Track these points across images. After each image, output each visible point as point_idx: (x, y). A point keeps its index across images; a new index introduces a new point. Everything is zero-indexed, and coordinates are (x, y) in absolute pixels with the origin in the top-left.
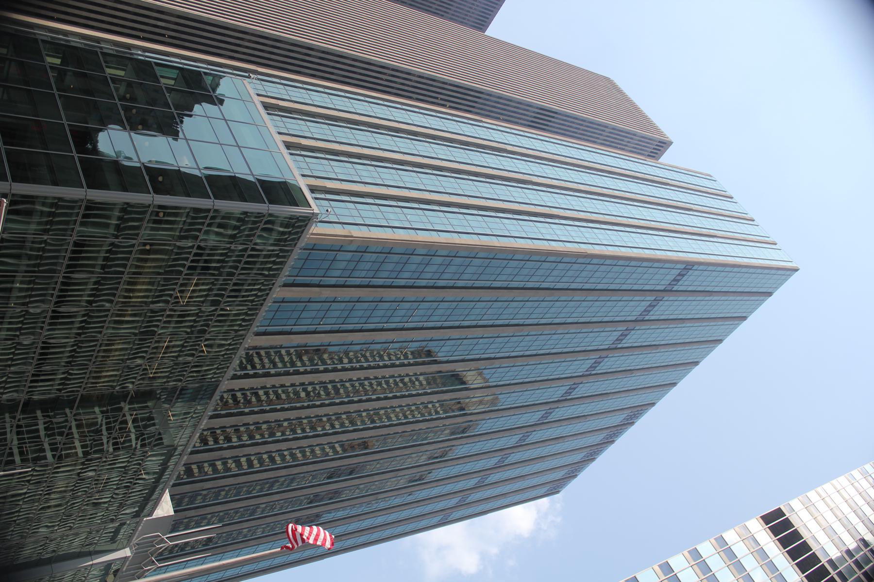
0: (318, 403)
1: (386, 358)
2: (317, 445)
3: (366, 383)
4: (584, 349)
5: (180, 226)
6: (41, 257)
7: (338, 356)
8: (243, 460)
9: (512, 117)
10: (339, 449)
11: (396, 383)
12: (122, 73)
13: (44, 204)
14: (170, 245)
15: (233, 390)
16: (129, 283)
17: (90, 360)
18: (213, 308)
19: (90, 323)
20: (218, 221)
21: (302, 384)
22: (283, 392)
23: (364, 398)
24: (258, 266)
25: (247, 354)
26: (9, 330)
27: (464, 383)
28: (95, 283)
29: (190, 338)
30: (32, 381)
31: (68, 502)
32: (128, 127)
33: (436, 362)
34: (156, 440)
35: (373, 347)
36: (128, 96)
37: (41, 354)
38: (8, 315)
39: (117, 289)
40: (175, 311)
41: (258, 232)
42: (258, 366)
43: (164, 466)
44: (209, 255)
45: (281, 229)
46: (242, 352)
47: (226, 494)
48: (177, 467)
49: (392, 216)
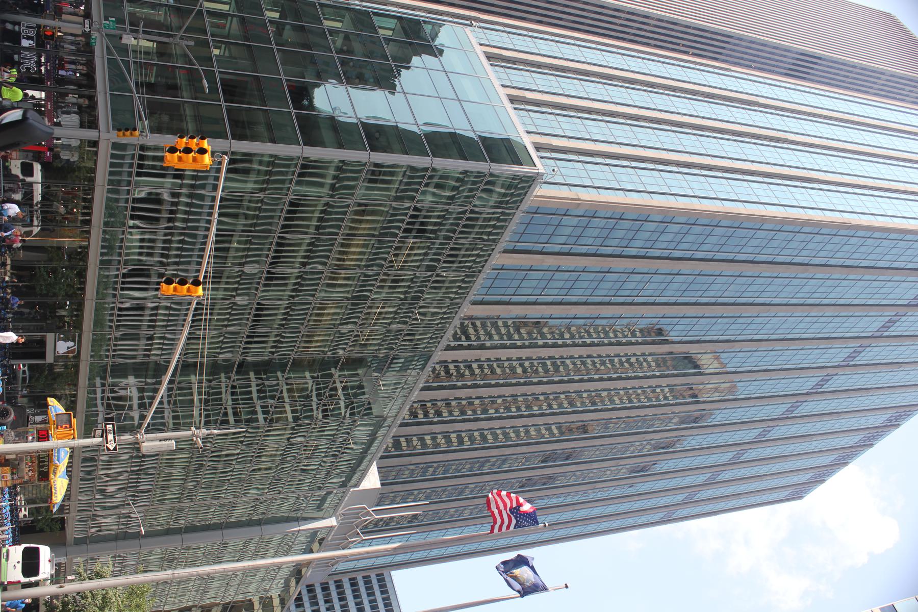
0: (535, 380)
1: (611, 335)
2: (533, 425)
3: (589, 361)
4: (841, 335)
5: (397, 186)
6: (257, 217)
7: (560, 330)
8: (453, 436)
9: (766, 64)
10: (555, 431)
11: (621, 363)
12: (339, 25)
13: (261, 163)
14: (385, 206)
15: (446, 362)
16: (343, 245)
17: (302, 324)
18: (430, 273)
19: (302, 285)
20: (435, 180)
21: (520, 359)
22: (499, 366)
23: (586, 377)
24: (476, 230)
25: (462, 324)
26: (226, 289)
27: (697, 367)
28: (309, 244)
29: (403, 304)
30: (247, 343)
31: (277, 466)
32: (344, 81)
33: (666, 342)
34: (366, 410)
35: (598, 322)
36: (345, 48)
37: (255, 315)
38: (225, 274)
39: (330, 251)
40: (388, 275)
41: (479, 194)
42: (473, 338)
43: (373, 437)
44: (425, 217)
45: (503, 191)
46: (457, 322)
47: (434, 471)
48: (385, 439)
49: (624, 178)
